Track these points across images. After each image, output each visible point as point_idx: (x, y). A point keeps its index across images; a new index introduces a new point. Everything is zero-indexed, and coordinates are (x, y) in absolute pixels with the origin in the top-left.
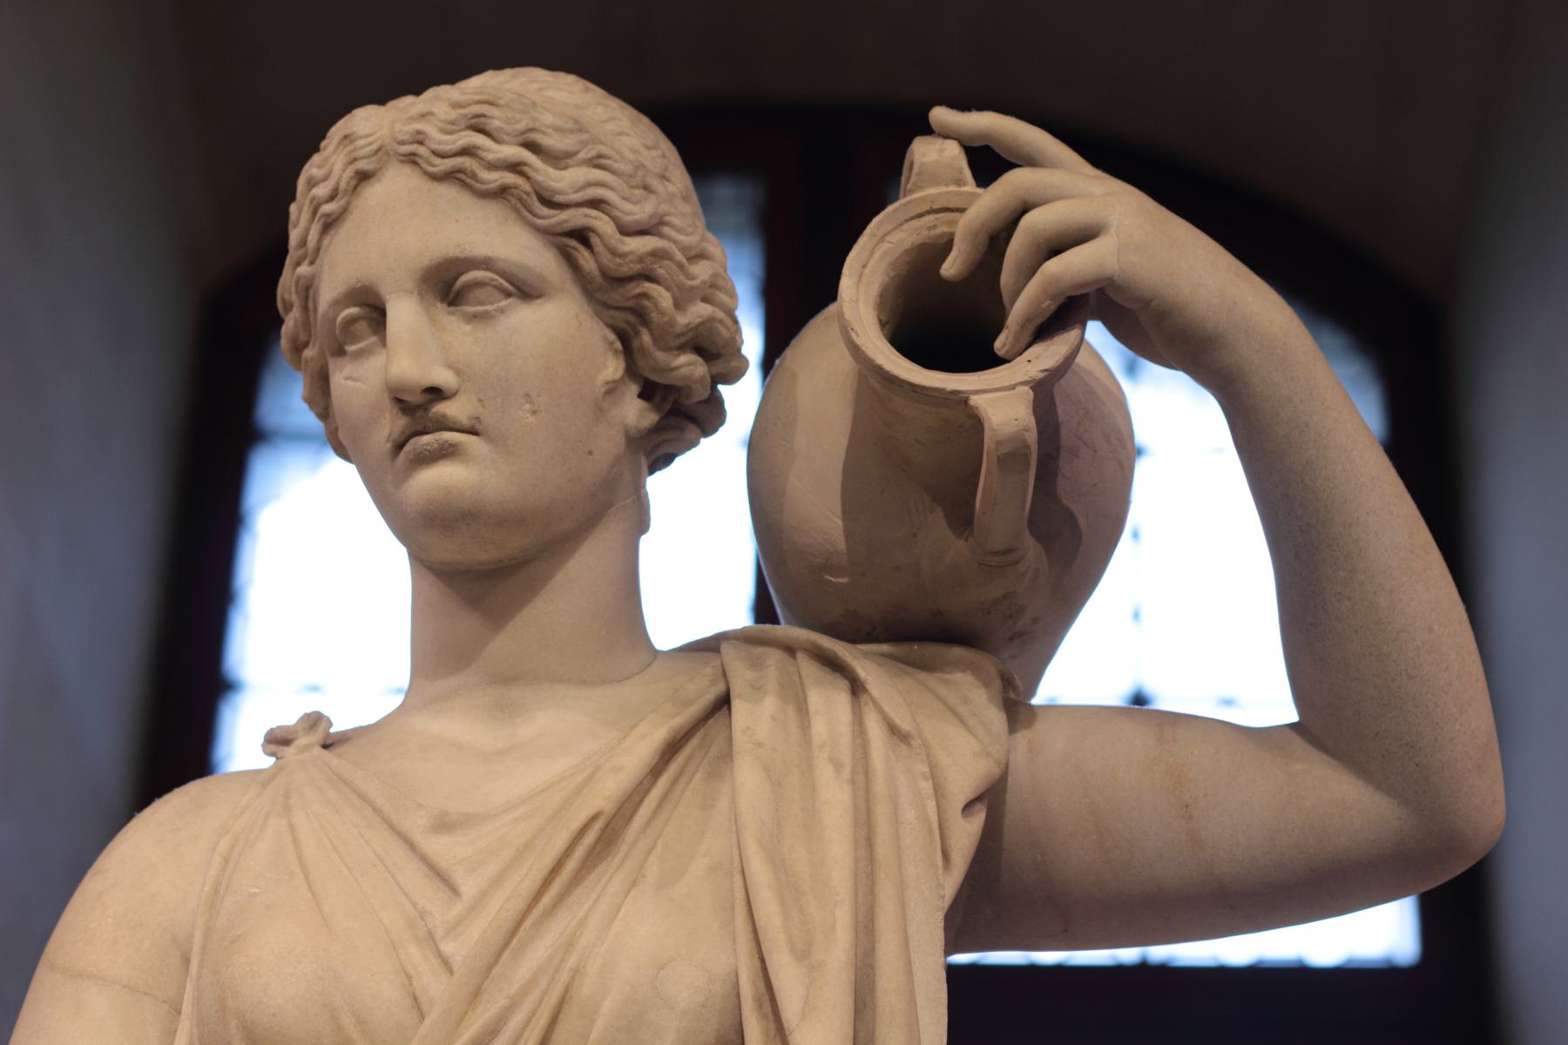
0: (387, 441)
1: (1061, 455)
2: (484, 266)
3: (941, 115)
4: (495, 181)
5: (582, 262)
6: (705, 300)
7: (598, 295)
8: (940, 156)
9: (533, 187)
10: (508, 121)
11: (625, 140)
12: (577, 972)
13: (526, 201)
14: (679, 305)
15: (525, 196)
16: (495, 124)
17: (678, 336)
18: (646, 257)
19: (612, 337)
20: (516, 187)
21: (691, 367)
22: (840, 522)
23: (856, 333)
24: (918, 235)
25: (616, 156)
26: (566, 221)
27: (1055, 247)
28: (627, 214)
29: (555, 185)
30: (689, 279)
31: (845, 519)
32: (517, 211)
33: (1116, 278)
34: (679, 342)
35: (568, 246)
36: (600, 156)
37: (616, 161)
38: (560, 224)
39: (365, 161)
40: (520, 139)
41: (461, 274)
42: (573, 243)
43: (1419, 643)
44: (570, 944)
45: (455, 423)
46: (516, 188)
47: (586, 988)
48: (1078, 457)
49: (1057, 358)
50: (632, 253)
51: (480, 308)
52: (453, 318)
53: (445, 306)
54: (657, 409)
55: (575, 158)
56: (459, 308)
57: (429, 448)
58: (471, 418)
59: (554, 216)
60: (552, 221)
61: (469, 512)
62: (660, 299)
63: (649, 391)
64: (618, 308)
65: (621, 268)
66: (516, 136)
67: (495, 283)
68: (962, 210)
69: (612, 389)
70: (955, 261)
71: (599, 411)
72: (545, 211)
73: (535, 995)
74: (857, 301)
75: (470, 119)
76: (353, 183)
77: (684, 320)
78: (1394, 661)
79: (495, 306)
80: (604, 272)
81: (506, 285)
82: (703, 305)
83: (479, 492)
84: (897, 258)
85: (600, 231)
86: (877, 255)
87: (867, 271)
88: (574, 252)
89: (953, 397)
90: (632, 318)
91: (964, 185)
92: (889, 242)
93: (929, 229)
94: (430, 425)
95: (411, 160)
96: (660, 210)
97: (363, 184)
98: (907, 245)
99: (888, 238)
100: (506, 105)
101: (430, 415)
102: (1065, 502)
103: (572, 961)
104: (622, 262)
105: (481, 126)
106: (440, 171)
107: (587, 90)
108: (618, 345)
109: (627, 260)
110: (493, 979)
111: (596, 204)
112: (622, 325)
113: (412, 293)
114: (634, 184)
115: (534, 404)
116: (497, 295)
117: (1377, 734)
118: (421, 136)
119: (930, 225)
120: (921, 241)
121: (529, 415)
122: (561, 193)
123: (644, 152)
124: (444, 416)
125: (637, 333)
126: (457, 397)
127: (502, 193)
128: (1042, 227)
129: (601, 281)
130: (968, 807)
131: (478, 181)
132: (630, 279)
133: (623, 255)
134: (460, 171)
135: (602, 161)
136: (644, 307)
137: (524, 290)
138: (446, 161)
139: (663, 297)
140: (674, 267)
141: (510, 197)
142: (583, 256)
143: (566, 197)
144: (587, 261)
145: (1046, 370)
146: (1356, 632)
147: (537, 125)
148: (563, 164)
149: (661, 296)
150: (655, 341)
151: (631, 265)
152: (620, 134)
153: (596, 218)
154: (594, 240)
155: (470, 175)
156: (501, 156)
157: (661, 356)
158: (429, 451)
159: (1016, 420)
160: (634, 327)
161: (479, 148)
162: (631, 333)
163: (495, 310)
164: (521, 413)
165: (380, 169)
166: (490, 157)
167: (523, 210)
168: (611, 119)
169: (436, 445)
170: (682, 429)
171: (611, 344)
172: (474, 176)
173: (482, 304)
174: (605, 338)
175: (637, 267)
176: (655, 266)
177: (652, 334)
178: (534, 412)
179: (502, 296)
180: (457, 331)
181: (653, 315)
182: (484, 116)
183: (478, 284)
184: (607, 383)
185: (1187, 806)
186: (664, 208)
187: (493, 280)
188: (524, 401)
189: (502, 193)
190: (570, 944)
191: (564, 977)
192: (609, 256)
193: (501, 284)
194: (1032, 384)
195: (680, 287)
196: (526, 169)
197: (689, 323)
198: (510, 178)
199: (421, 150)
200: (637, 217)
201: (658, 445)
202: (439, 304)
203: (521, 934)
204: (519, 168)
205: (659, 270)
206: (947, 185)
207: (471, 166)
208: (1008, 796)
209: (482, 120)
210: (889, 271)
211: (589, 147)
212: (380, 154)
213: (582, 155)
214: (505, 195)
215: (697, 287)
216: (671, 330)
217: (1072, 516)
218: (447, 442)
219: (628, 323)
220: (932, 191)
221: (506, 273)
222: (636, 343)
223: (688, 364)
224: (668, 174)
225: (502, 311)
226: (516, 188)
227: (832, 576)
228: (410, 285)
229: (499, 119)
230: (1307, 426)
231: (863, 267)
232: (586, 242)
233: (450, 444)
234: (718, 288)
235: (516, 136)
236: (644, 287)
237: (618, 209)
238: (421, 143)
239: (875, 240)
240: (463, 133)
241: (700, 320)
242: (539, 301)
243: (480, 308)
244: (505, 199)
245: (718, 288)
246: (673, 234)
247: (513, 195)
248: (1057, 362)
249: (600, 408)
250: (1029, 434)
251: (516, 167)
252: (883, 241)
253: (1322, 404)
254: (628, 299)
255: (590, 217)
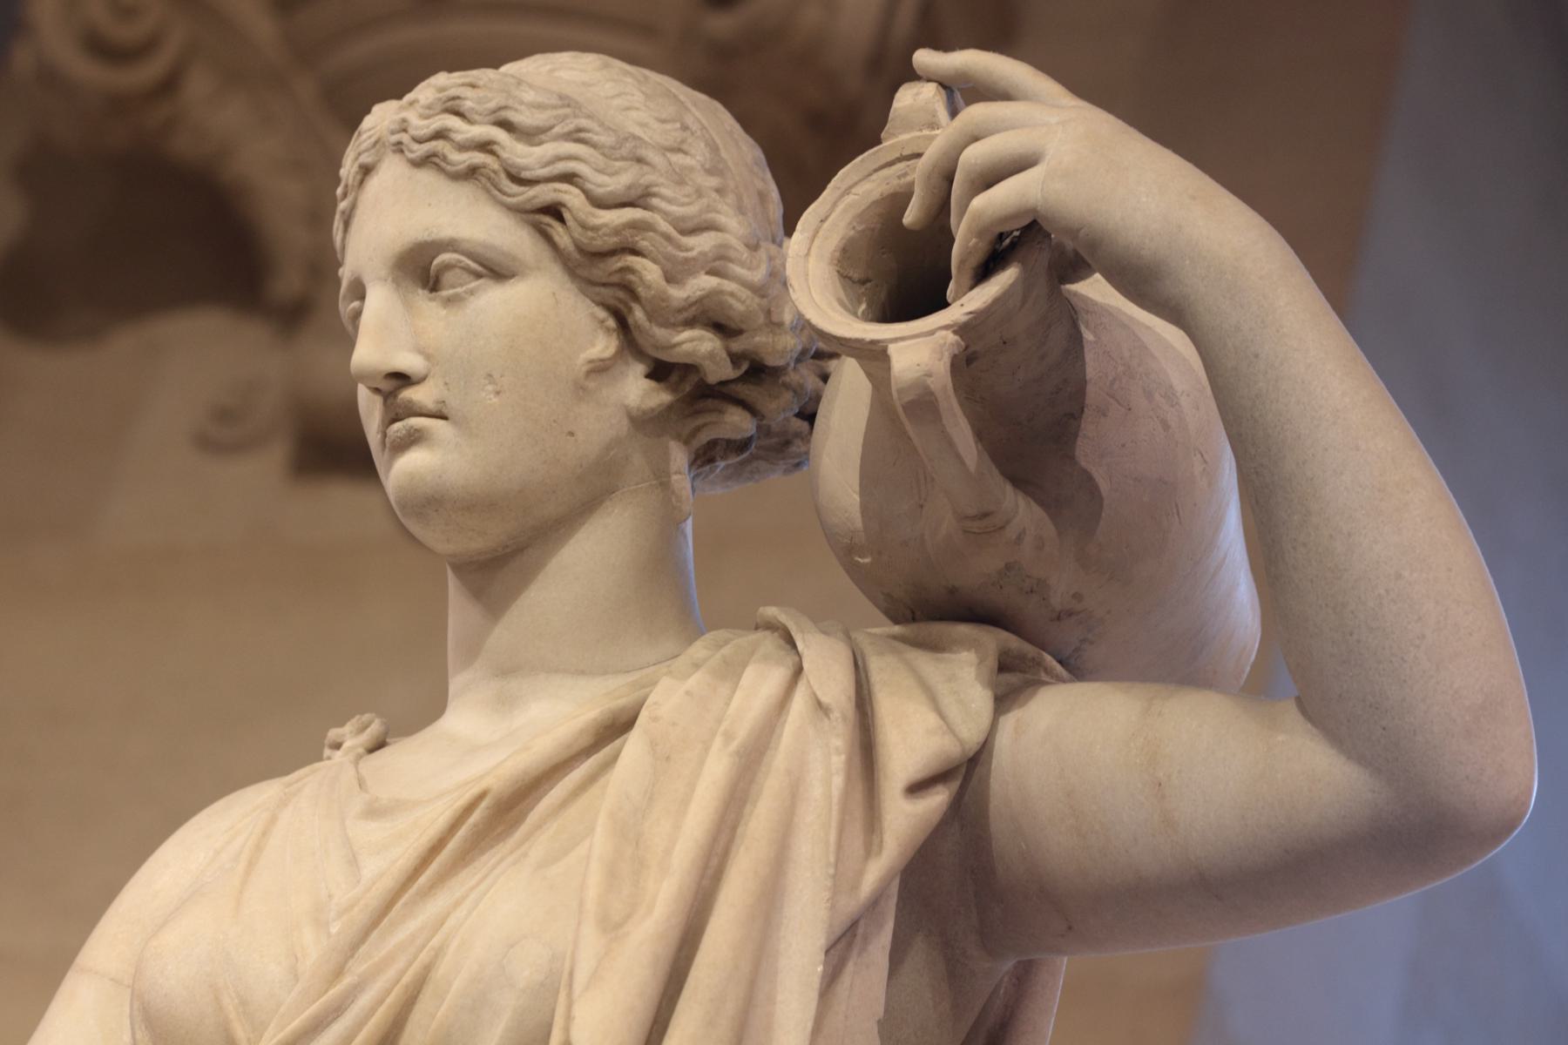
0: (378, 433)
1: (1084, 416)
2: (450, 248)
3: (924, 58)
4: (465, 161)
5: (556, 238)
6: (713, 272)
7: (579, 271)
8: (915, 100)
9: (501, 165)
10: (479, 101)
11: (634, 114)
12: (439, 953)
13: (494, 180)
14: (670, 279)
15: (492, 175)
16: (467, 105)
17: (680, 311)
18: (624, 229)
19: (602, 314)
20: (484, 166)
21: (695, 343)
22: (857, 498)
23: (794, 290)
24: (888, 184)
25: (597, 129)
26: (534, 197)
27: (990, 178)
28: (599, 186)
29: (519, 161)
30: (682, 251)
31: (861, 496)
32: (488, 191)
33: (1039, 208)
34: (681, 317)
35: (541, 223)
36: (580, 130)
37: (597, 134)
38: (529, 200)
39: (366, 154)
40: (492, 118)
41: (434, 258)
42: (547, 219)
43: (1382, 592)
44: (441, 921)
45: (420, 408)
46: (485, 167)
47: (441, 970)
48: (1105, 415)
49: (984, 299)
50: (605, 225)
51: (451, 292)
52: (433, 304)
53: (426, 292)
54: (674, 389)
55: (549, 134)
56: (439, 293)
57: (399, 434)
58: (438, 402)
59: (523, 193)
60: (520, 198)
61: (433, 497)
62: (644, 272)
63: (660, 372)
64: (604, 285)
65: (594, 242)
66: (486, 115)
67: (462, 265)
68: (919, 155)
69: (600, 369)
70: (911, 211)
71: (580, 390)
72: (515, 188)
73: (391, 973)
74: (808, 254)
75: (445, 102)
76: (359, 177)
77: (678, 294)
78: (1352, 612)
79: (464, 288)
80: (580, 249)
81: (479, 269)
82: (707, 278)
83: (440, 477)
84: (864, 211)
85: (569, 205)
86: (841, 207)
87: (826, 225)
88: (549, 229)
89: (874, 348)
90: (621, 294)
91: (938, 129)
92: (855, 194)
93: (899, 177)
94: (401, 411)
95: (399, 148)
96: (642, 181)
97: (367, 178)
98: (876, 196)
99: (853, 190)
100: (485, 86)
101: (398, 401)
102: (1083, 464)
103: (435, 942)
104: (595, 235)
105: (457, 109)
106: (417, 157)
107: (606, 66)
108: (611, 323)
109: (600, 233)
110: (358, 957)
111: (569, 178)
112: (612, 302)
113: (386, 280)
114: (618, 156)
115: (497, 384)
116: (465, 276)
117: (1340, 696)
118: (405, 124)
119: (900, 173)
120: (892, 191)
121: (492, 396)
122: (526, 168)
123: (656, 125)
124: (410, 401)
125: (630, 310)
126: (427, 380)
127: (472, 173)
128: (973, 161)
129: (578, 256)
130: (917, 788)
131: (448, 164)
132: (612, 253)
133: (595, 229)
134: (435, 155)
135: (582, 135)
136: (630, 282)
137: (495, 270)
138: (422, 145)
139: (649, 272)
140: (658, 238)
141: (480, 178)
142: (558, 233)
143: (533, 172)
144: (561, 236)
145: (971, 313)
146: (1312, 581)
147: (510, 102)
148: (537, 140)
149: (646, 269)
150: (651, 317)
151: (605, 238)
152: (628, 109)
153: (566, 192)
154: (567, 215)
155: (442, 157)
156: (469, 135)
157: (660, 333)
158: (400, 438)
159: (918, 365)
160: (626, 305)
161: (450, 130)
162: (625, 310)
163: (466, 292)
164: (484, 394)
165: (379, 161)
166: (458, 137)
167: (492, 188)
168: (619, 95)
169: (404, 432)
170: (721, 412)
171: (602, 322)
172: (445, 158)
173: (453, 287)
174: (593, 316)
175: (613, 241)
176: (637, 239)
177: (643, 307)
178: (498, 393)
179: (472, 277)
180: (431, 313)
181: (640, 289)
182: (458, 98)
183: (448, 267)
184: (591, 362)
185: (1160, 784)
186: (650, 178)
187: (461, 262)
188: (487, 382)
189: (472, 173)
190: (441, 921)
191: (424, 957)
192: (580, 229)
193: (468, 265)
194: (955, 328)
195: (669, 258)
196: (495, 148)
197: (689, 297)
198: (478, 158)
199: (405, 138)
200: (609, 189)
201: (698, 430)
202: (420, 291)
203: (392, 914)
204: (489, 147)
205: (641, 242)
206: (921, 130)
207: (443, 149)
208: (992, 780)
209: (457, 102)
210: (855, 224)
211: (568, 121)
212: (378, 146)
213: (557, 130)
214: (476, 176)
215: (694, 259)
216: (664, 304)
217: (1090, 478)
218: (412, 427)
219: (620, 301)
220: (905, 137)
221: (471, 253)
222: (630, 321)
223: (692, 340)
224: (685, 147)
225: (472, 292)
226: (485, 167)
227: (860, 557)
228: (383, 273)
229: (471, 100)
230: (1257, 356)
231: (822, 221)
232: (561, 219)
233: (416, 430)
234: (731, 260)
235: (486, 115)
236: (626, 261)
237: (589, 182)
238: (405, 130)
239: (838, 193)
240: (437, 118)
241: (703, 293)
242: (512, 281)
243: (451, 292)
244: (476, 179)
245: (731, 260)
246: (663, 205)
247: (483, 175)
248: (985, 303)
249: (582, 388)
250: (932, 379)
251: (486, 146)
252: (848, 194)
253: (1278, 331)
254: (610, 274)
255: (560, 191)
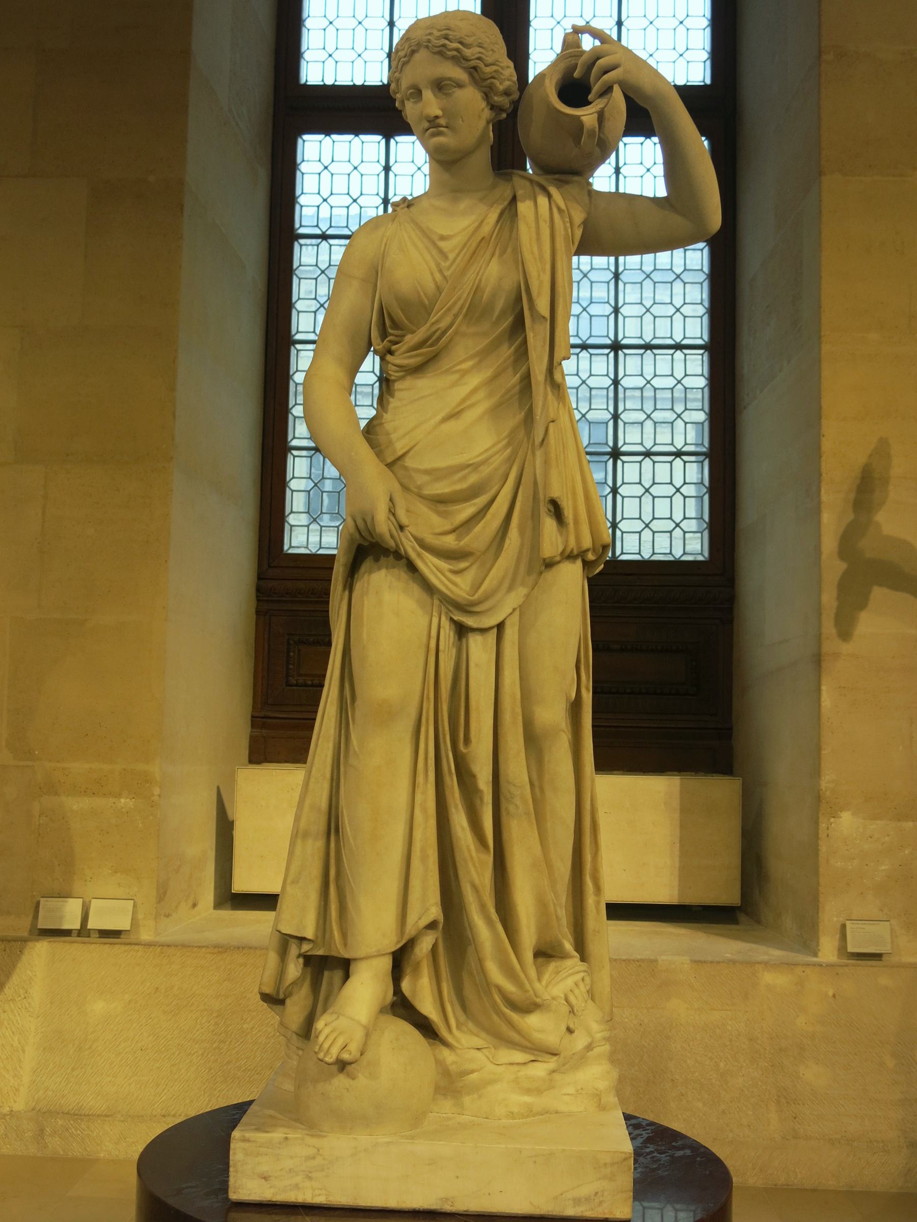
12: (480, 281)
19: (483, 95)
42: (472, 70)
69: (483, 110)
90: (488, 89)
93: (569, 62)
95: (427, 47)
125: (490, 93)
137: (460, 85)
154: (478, 69)
156: (452, 47)
166: (450, 47)
172: (445, 53)
175: (490, 76)
183: (447, 85)
238: (430, 42)
251: (457, 50)
